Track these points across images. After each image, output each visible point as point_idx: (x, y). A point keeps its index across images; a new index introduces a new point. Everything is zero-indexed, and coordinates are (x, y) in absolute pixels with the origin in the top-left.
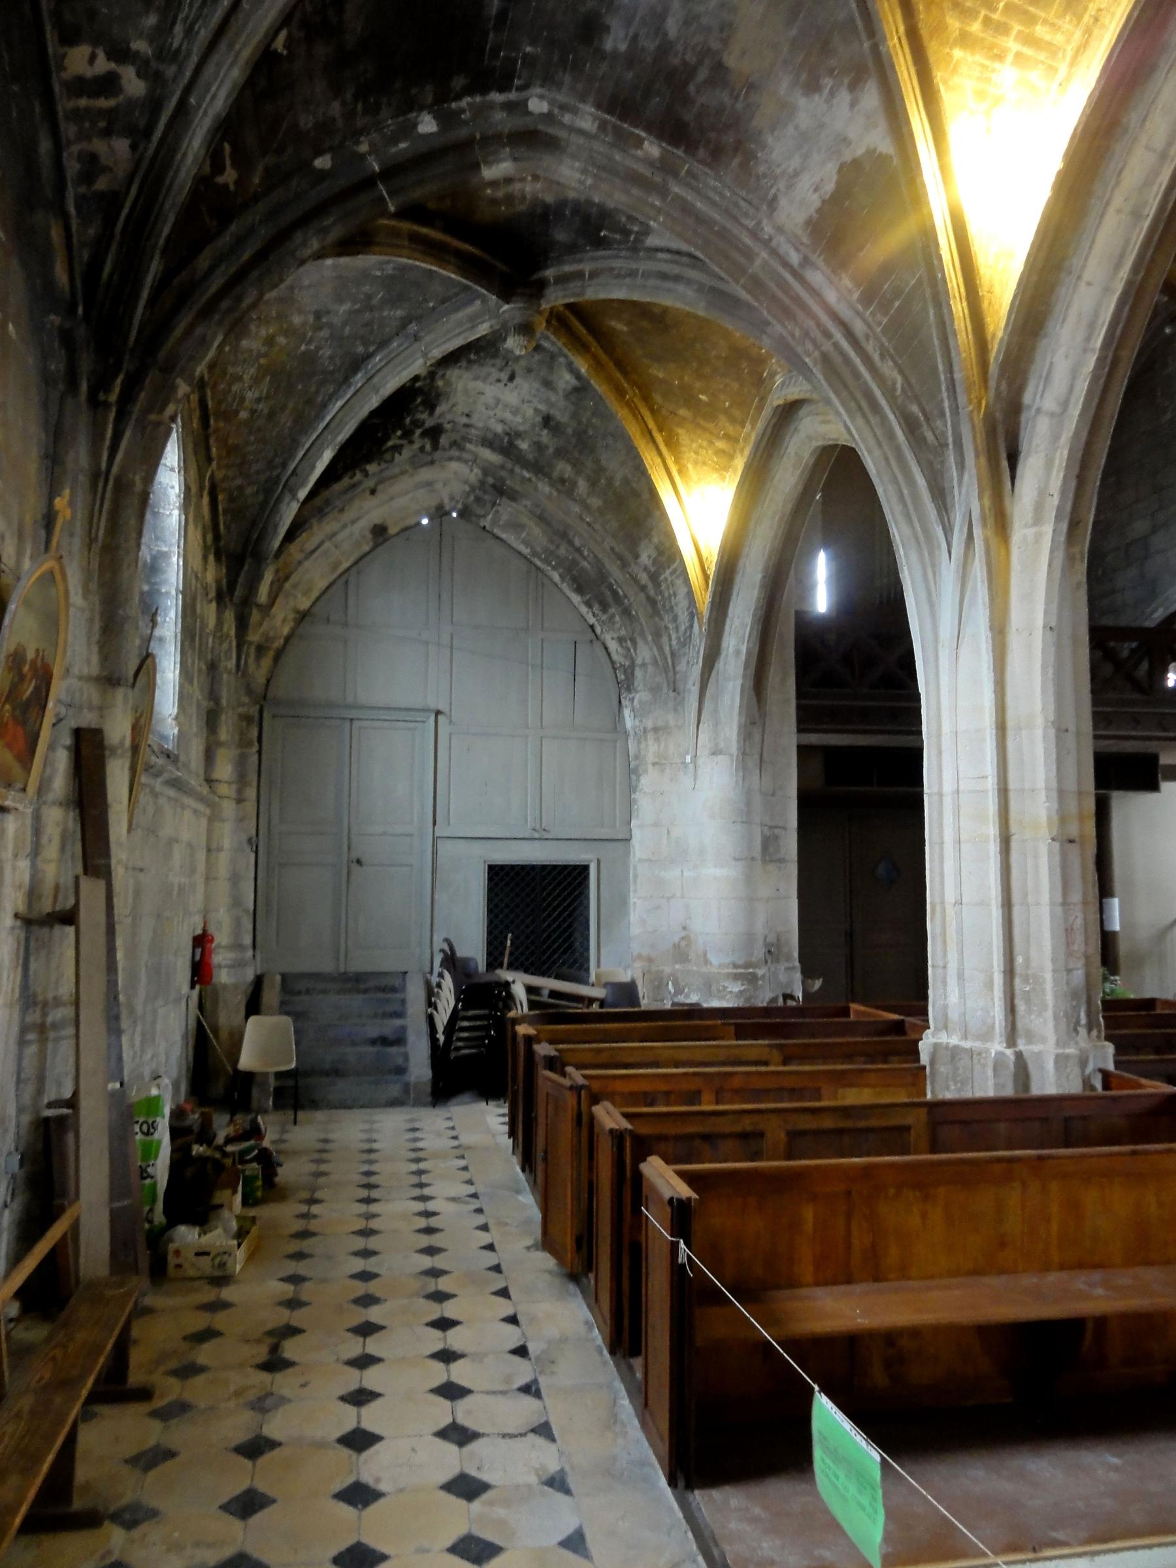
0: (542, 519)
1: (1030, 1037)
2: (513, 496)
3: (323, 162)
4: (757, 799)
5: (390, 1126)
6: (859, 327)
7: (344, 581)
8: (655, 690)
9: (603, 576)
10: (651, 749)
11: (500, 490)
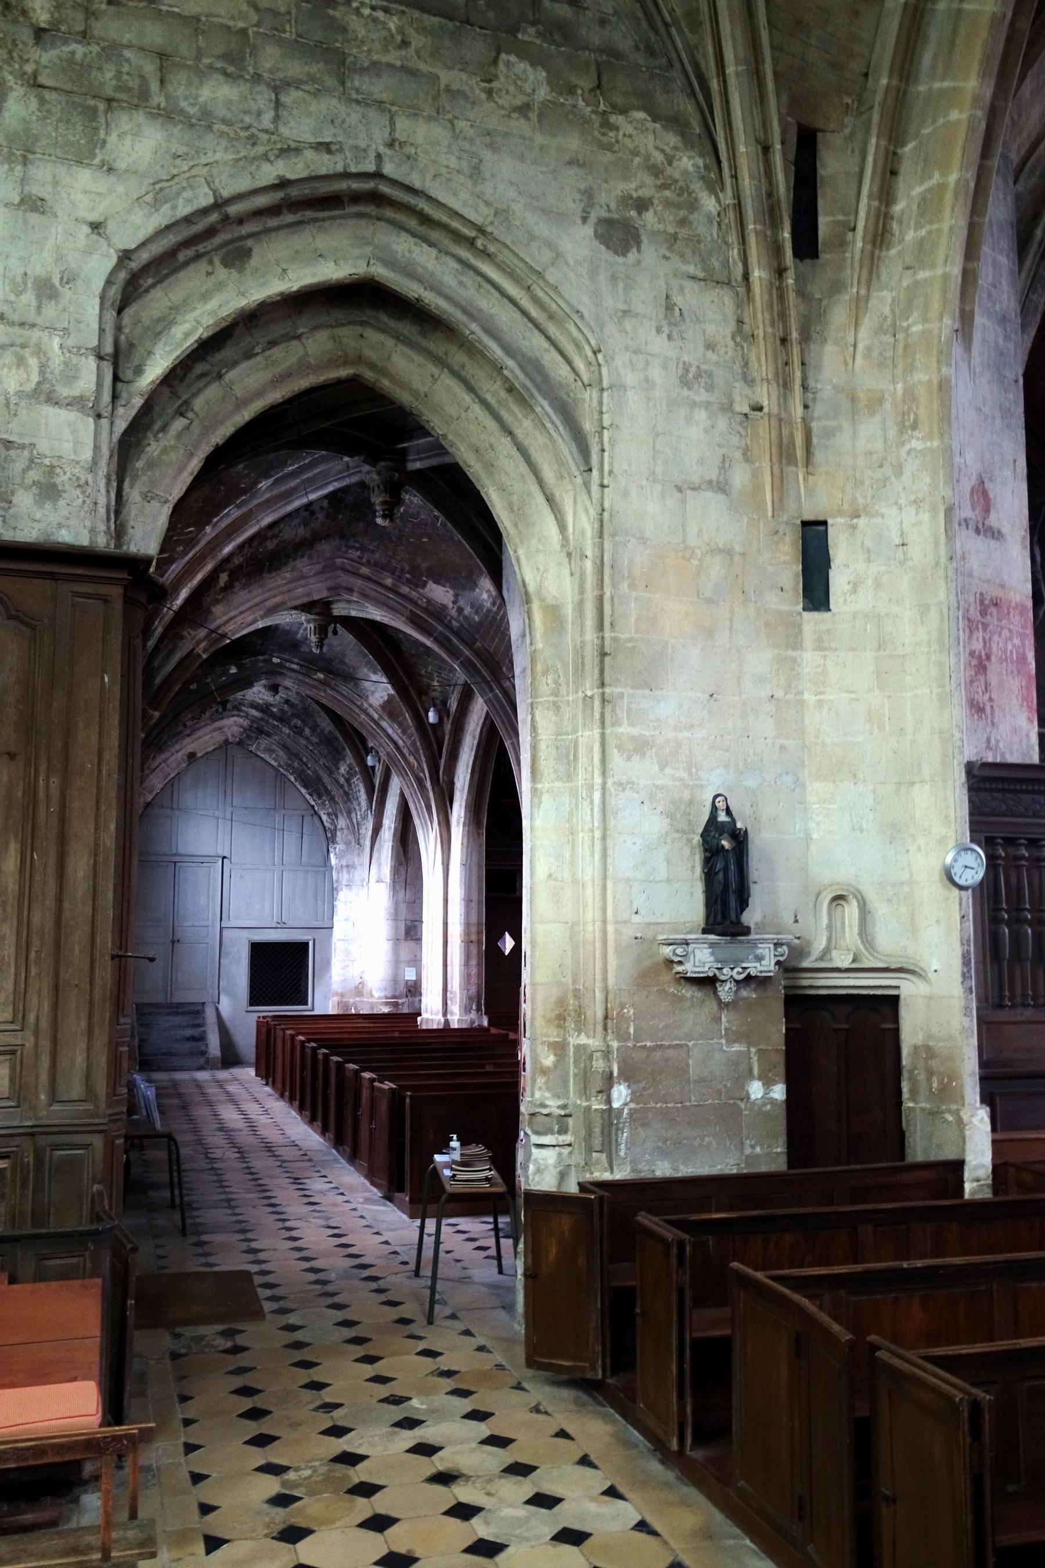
0: (284, 747)
1: (452, 1014)
2: (268, 735)
3: (193, 687)
4: (403, 908)
5: (203, 1076)
6: (400, 743)
7: (171, 784)
8: (348, 844)
9: (319, 779)
10: (344, 877)
11: (261, 731)
